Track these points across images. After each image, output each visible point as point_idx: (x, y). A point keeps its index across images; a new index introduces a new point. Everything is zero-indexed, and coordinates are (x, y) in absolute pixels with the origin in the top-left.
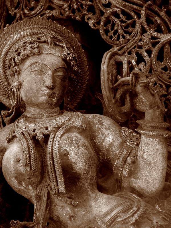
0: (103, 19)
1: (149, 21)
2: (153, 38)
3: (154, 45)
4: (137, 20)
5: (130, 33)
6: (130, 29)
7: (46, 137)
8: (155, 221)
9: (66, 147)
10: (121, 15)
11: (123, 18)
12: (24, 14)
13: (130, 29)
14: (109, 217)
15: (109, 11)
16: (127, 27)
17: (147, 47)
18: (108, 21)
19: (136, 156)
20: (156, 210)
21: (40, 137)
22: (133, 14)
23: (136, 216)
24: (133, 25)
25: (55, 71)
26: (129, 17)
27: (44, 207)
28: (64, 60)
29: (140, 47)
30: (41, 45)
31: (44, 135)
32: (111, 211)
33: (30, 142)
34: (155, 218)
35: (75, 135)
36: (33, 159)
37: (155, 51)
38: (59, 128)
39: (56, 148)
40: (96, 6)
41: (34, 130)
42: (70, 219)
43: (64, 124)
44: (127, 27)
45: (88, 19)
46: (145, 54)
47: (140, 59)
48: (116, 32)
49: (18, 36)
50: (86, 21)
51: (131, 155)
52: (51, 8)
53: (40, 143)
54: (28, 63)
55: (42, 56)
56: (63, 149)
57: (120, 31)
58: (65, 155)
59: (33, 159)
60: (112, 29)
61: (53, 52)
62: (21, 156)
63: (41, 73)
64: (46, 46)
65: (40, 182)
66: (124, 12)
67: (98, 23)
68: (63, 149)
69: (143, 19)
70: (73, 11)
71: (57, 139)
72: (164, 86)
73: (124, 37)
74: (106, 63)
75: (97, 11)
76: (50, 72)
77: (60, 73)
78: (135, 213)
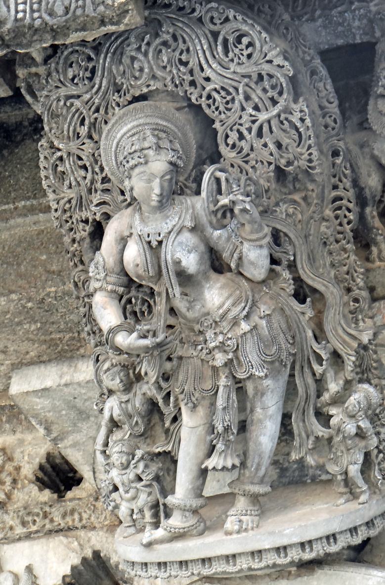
0: (205, 94)
1: (247, 98)
2: (251, 116)
3: (254, 122)
4: (236, 97)
5: (230, 110)
6: (229, 106)
7: (160, 243)
8: (262, 310)
9: (178, 255)
10: (221, 91)
11: (223, 93)
12: (131, 84)
13: (229, 106)
14: (221, 311)
15: (209, 87)
16: (227, 103)
17: (247, 126)
18: (209, 97)
19: (241, 253)
20: (264, 291)
21: (154, 244)
22: (231, 90)
23: (245, 313)
24: (233, 100)
25: (162, 177)
26: (229, 93)
27: (164, 300)
28: (171, 163)
29: (241, 125)
30: (146, 152)
31: (157, 241)
32: (224, 304)
33: (146, 246)
34: (262, 306)
35: (186, 236)
36: (150, 265)
37: (255, 127)
38: (170, 232)
39: (169, 257)
40: (196, 81)
41: (149, 236)
42: (188, 310)
43: (175, 226)
44: (227, 103)
45: (191, 94)
46: (245, 133)
47: (241, 137)
48: (217, 109)
49: (125, 129)
50: (189, 96)
51: (238, 251)
52: (154, 77)
53: (154, 248)
54: (137, 171)
55: (150, 164)
56: (175, 257)
57: (222, 108)
58: (178, 263)
59: (150, 265)
60: (214, 105)
61: (159, 158)
62: (138, 261)
63: (149, 181)
64: (151, 153)
65: (159, 279)
66: (223, 88)
67: (201, 97)
68: (175, 257)
69: (241, 97)
70: (176, 86)
71: (170, 243)
72: (265, 163)
73: (224, 113)
74: (205, 190)
75: (198, 85)
76: (158, 180)
77: (168, 177)
78: (244, 309)
